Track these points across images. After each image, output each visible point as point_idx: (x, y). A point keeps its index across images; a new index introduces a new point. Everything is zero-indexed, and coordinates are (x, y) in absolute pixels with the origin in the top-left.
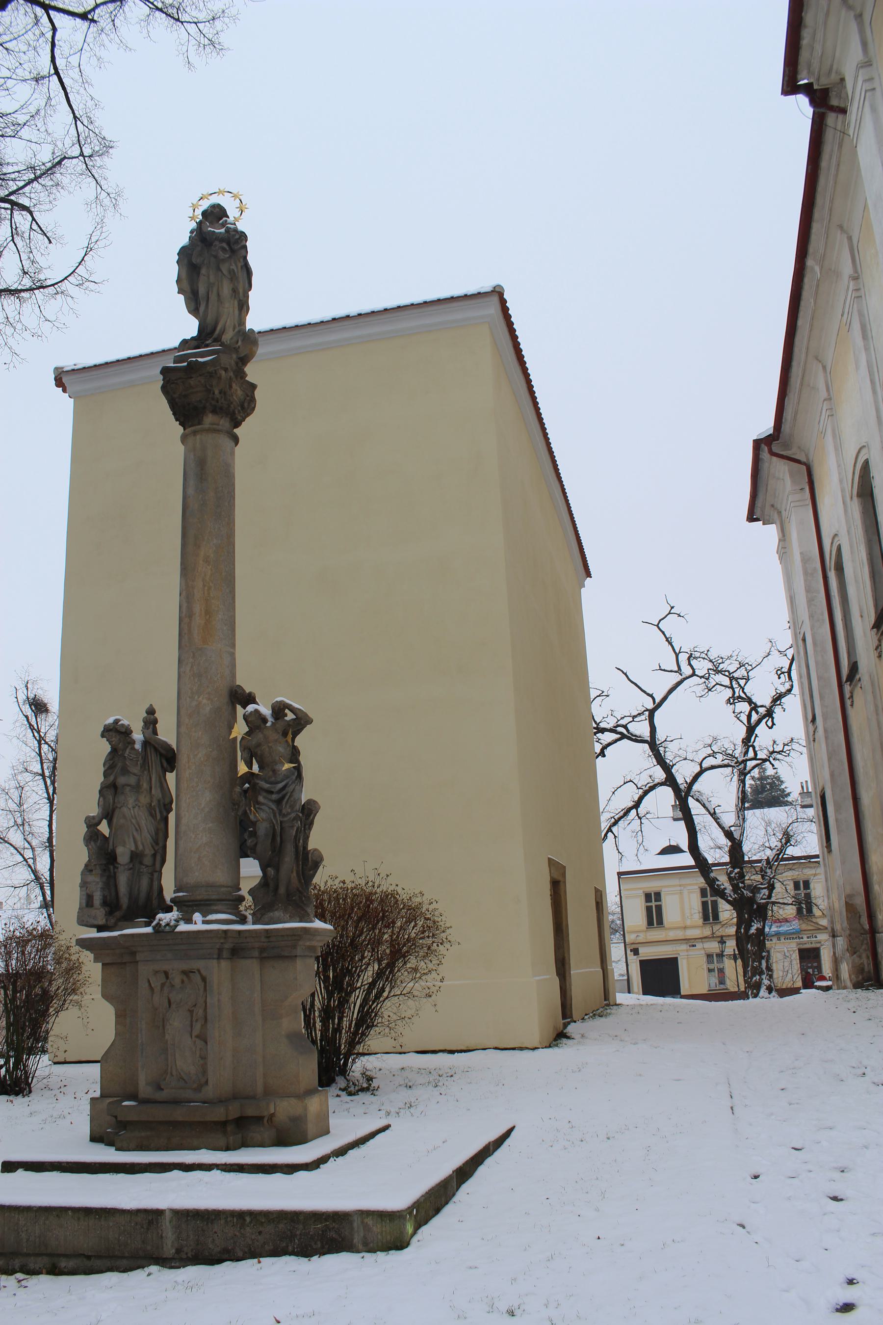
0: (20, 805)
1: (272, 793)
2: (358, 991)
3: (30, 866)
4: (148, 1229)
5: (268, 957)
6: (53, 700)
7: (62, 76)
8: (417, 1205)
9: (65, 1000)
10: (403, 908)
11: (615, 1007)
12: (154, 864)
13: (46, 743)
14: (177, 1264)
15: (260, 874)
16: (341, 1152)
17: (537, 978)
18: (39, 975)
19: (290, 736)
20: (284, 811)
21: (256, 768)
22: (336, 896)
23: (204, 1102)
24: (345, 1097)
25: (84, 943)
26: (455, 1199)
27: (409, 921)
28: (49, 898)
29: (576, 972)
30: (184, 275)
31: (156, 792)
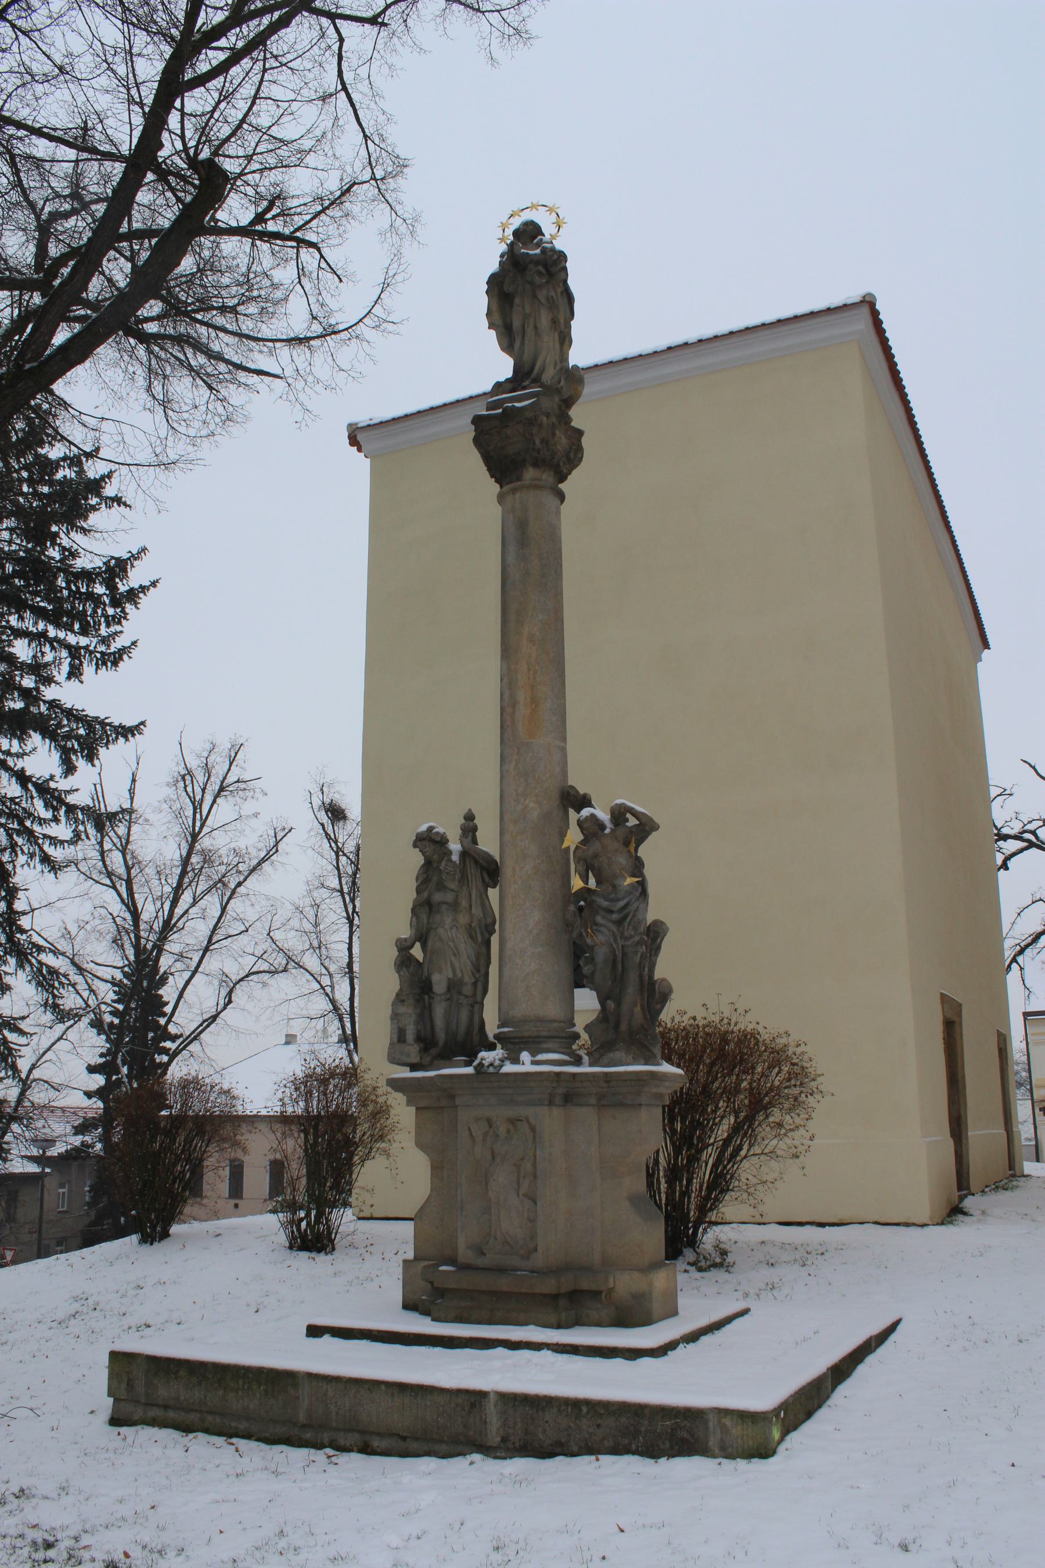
0: (316, 925)
1: (612, 912)
2: (710, 1148)
3: (327, 995)
4: (470, 1412)
5: (608, 1106)
6: (353, 805)
7: (350, 91)
8: (784, 1406)
9: (371, 1148)
10: (765, 1051)
11: (1023, 1179)
12: (474, 995)
13: (345, 855)
14: (503, 1454)
15: (598, 1007)
16: (692, 1337)
17: (927, 1140)
18: (341, 1119)
19: (633, 845)
20: (626, 934)
21: (592, 883)
22: (686, 1034)
23: (533, 1272)
24: (694, 1273)
25: (396, 1084)
26: (829, 1402)
27: (771, 1067)
28: (349, 1032)
29: (974, 1133)
31: (477, 911)
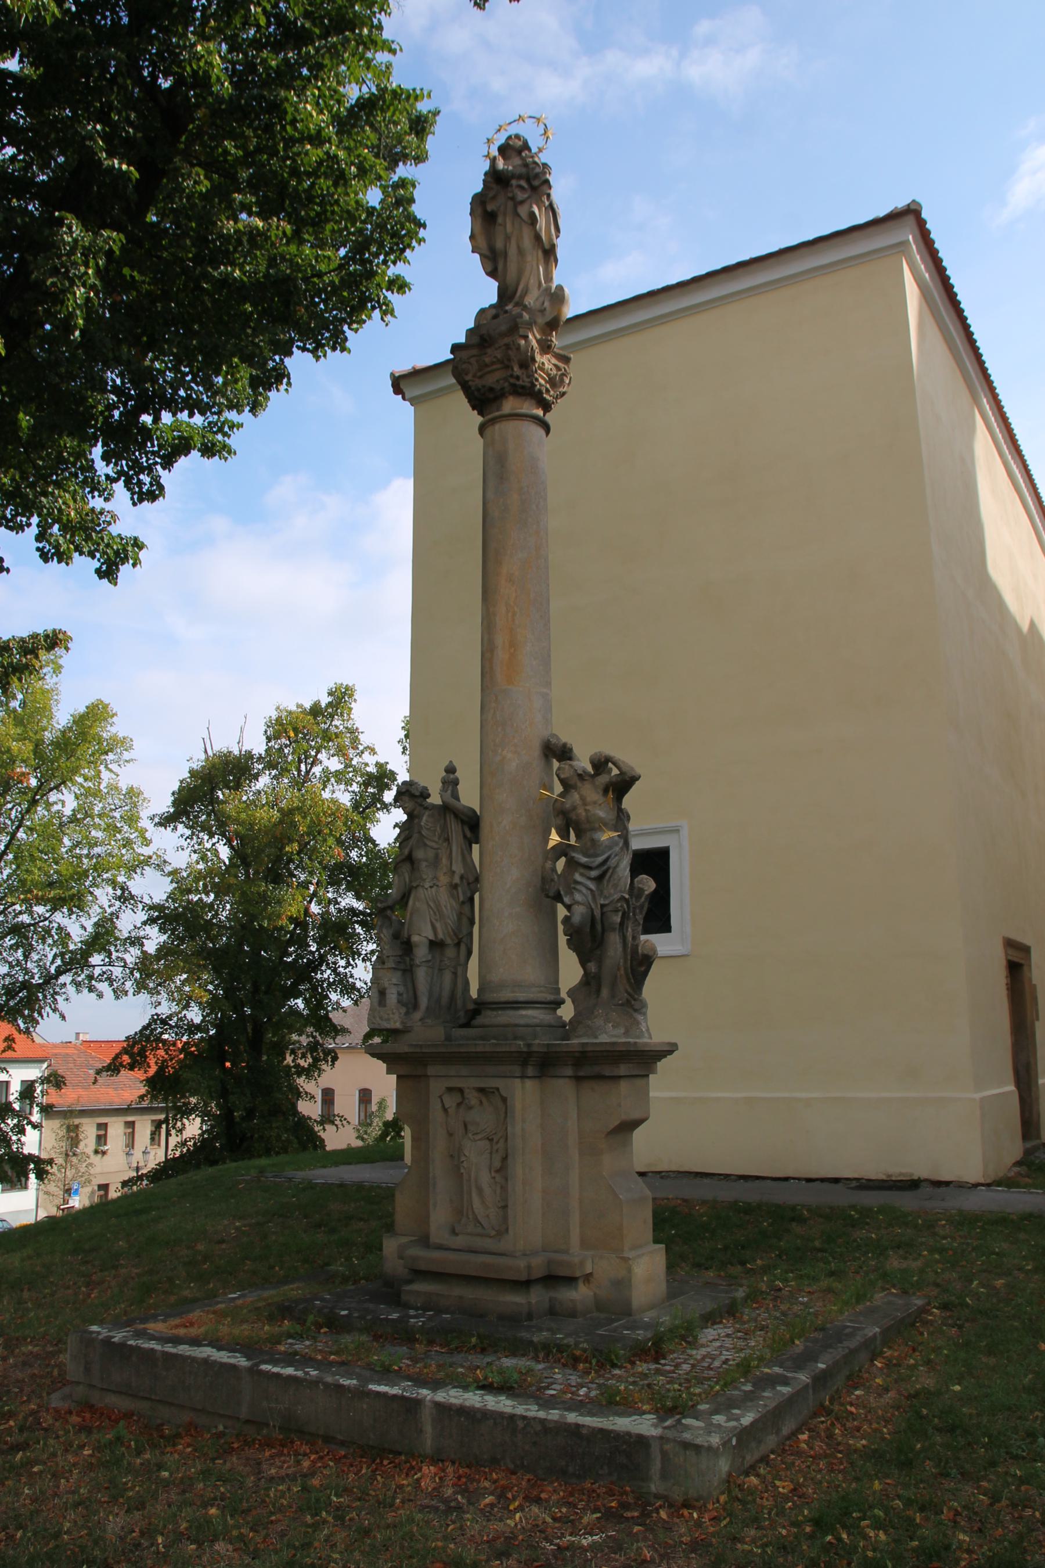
21: (573, 840)
30: (477, 231)
